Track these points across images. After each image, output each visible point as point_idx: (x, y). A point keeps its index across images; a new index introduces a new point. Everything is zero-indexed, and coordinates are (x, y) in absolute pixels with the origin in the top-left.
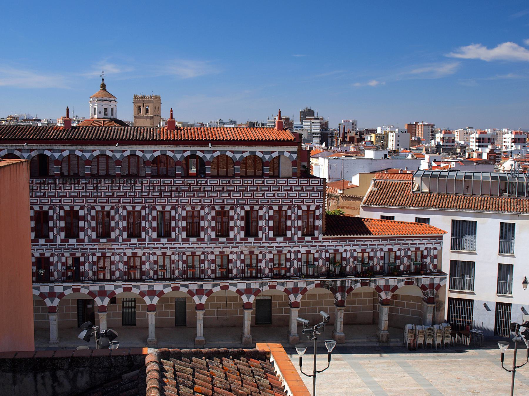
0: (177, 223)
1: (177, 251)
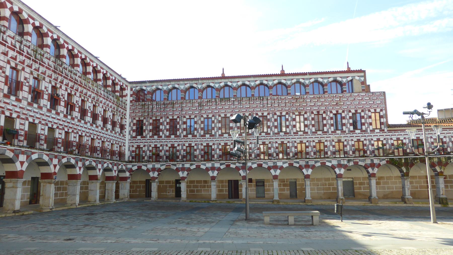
0: (290, 123)
1: (290, 140)
